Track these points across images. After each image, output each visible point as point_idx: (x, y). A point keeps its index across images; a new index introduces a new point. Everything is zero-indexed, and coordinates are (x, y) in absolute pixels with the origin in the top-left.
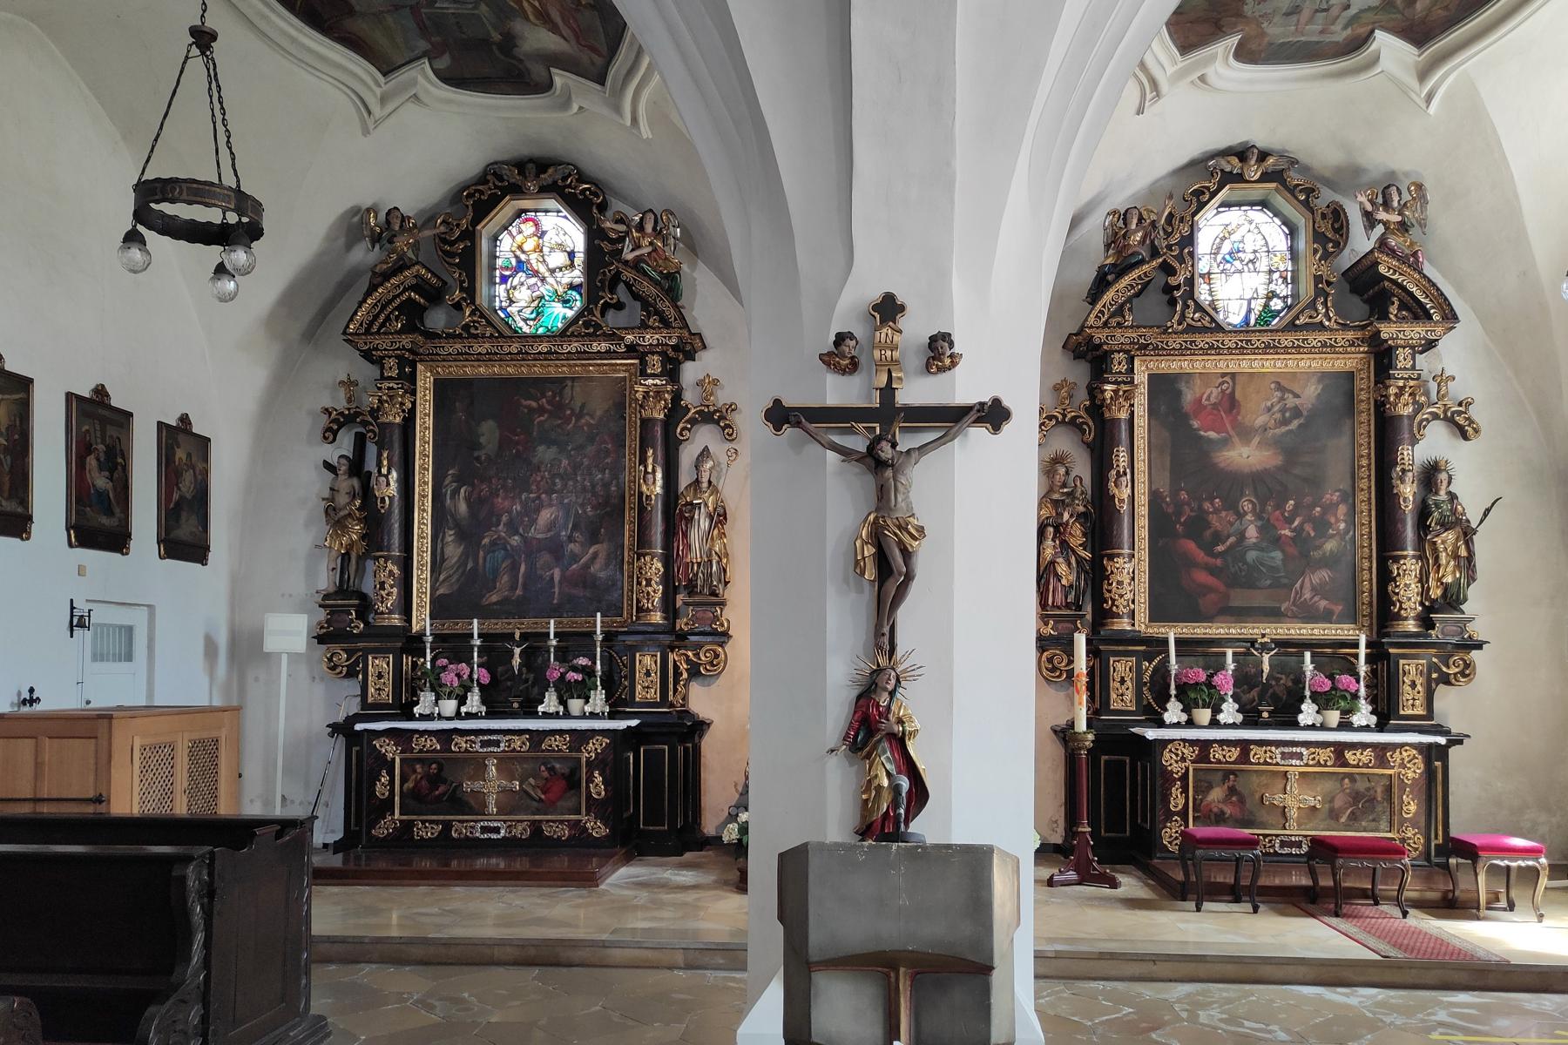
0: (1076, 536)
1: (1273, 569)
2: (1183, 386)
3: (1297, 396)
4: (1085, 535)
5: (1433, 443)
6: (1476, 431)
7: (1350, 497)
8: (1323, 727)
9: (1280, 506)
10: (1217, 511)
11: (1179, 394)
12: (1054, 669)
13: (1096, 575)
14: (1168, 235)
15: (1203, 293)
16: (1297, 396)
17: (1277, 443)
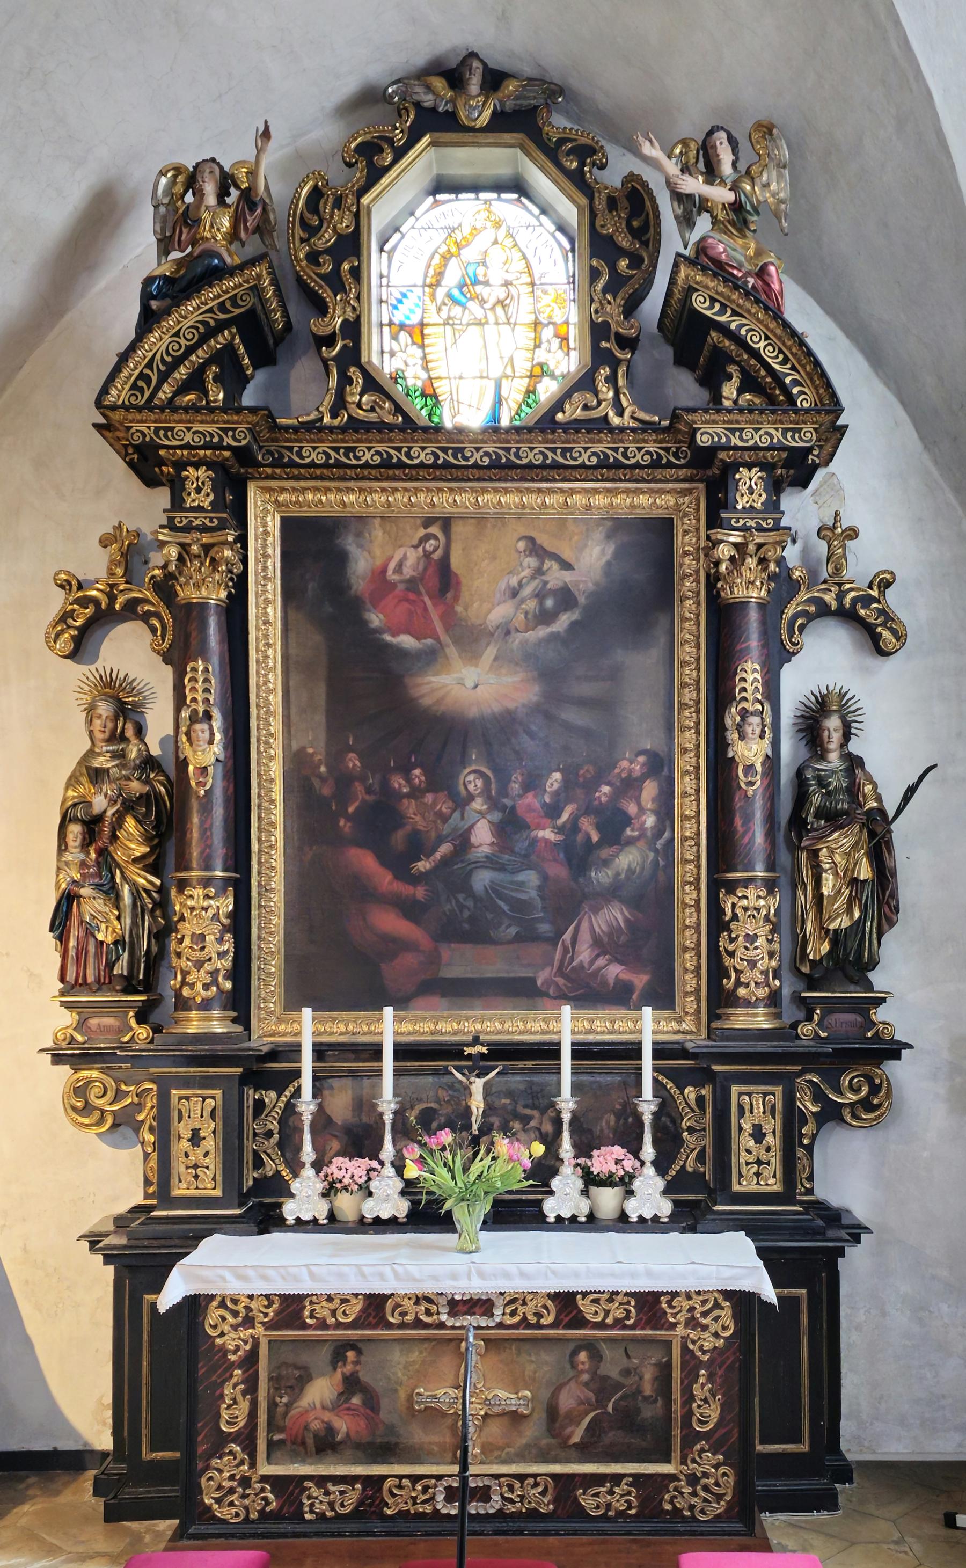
2: (350, 544)
3: (566, 566)
4: (148, 839)
5: (822, 661)
6: (900, 636)
10: (416, 793)
11: (341, 559)
14: (312, 231)
15: (388, 354)
16: (566, 566)
17: (529, 658)
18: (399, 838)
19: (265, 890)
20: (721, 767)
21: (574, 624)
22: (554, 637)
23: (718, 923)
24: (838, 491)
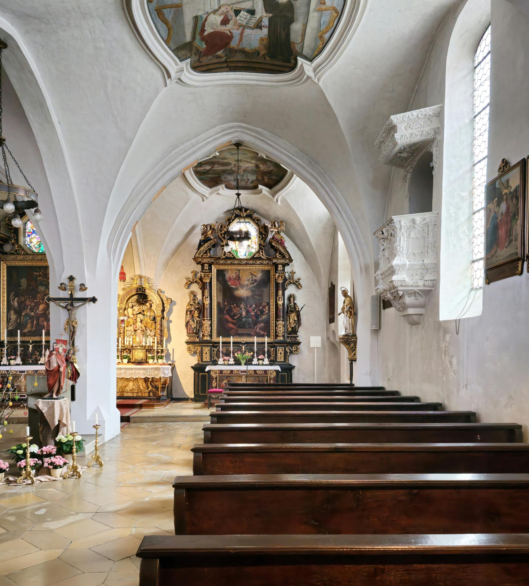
0: (196, 314)
1: (249, 323)
2: (226, 273)
3: (255, 276)
7: (268, 304)
8: (259, 365)
9: (251, 306)
10: (235, 307)
11: (225, 275)
12: (190, 350)
13: (200, 324)
16: (255, 276)
17: (250, 289)
18: (232, 314)
19: (214, 321)
20: (277, 304)
21: (257, 285)
22: (254, 286)
23: (276, 326)
24: (293, 266)
